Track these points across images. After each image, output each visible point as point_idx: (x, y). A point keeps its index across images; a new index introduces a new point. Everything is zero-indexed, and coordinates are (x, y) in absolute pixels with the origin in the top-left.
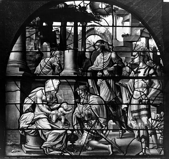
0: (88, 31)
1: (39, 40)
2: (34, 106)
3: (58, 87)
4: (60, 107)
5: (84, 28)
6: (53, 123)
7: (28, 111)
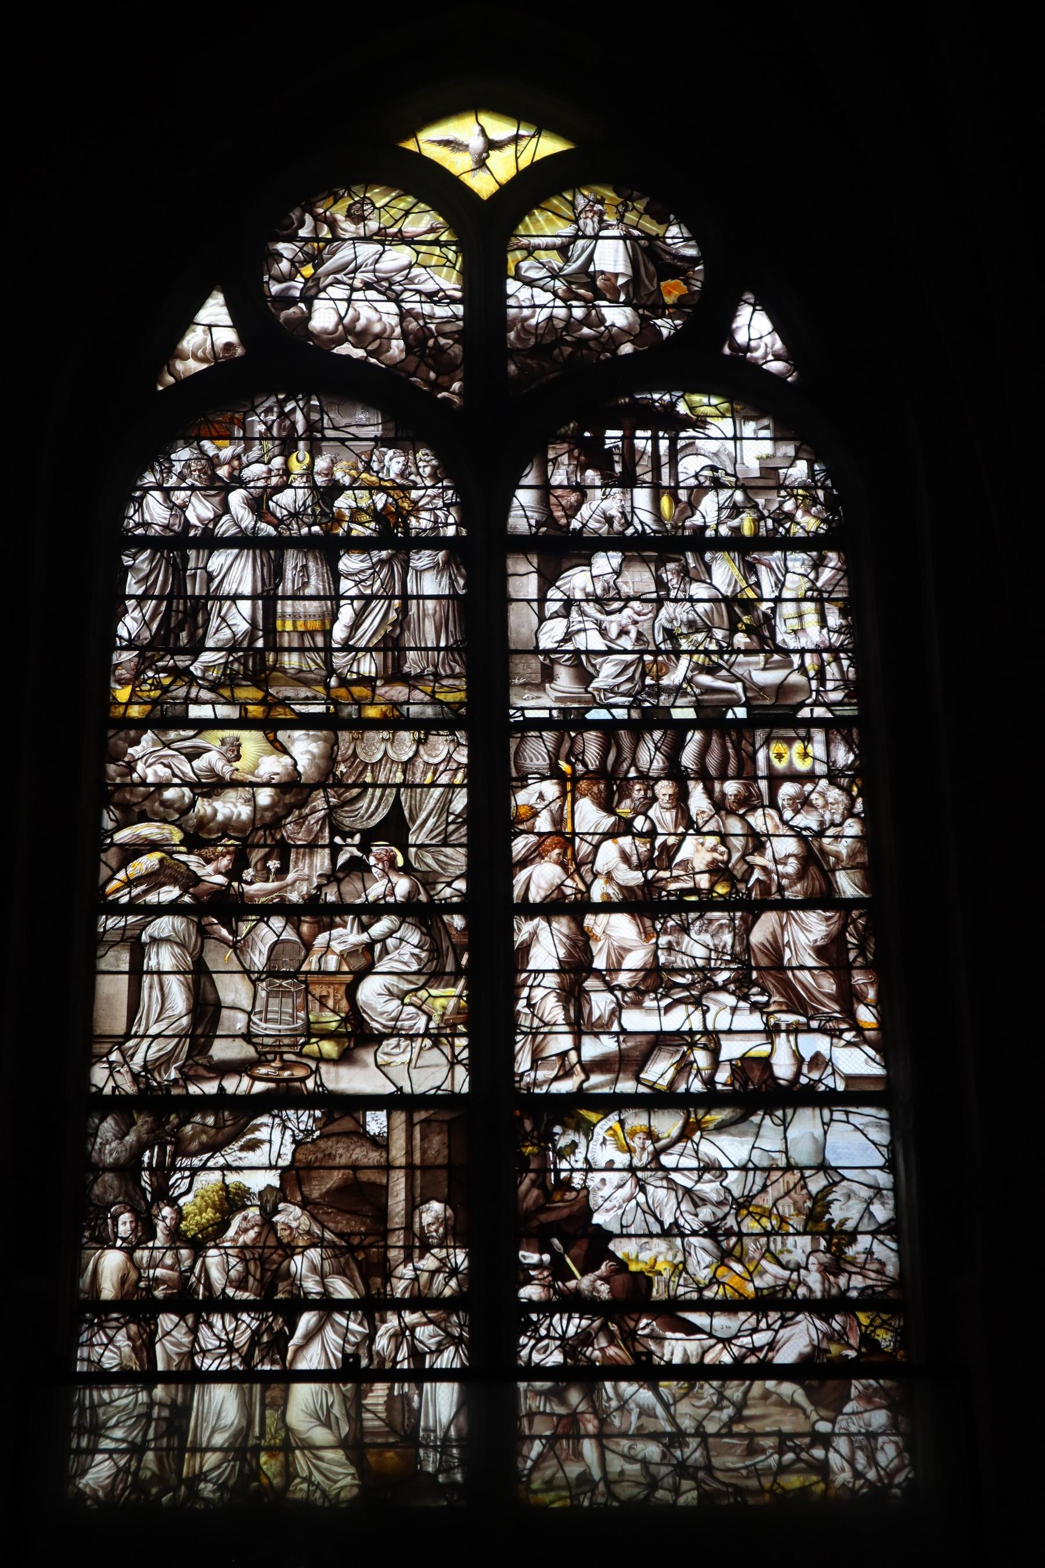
0: (683, 448)
1: (576, 466)
2: (569, 603)
3: (621, 565)
4: (625, 606)
6: (612, 641)
7: (556, 615)
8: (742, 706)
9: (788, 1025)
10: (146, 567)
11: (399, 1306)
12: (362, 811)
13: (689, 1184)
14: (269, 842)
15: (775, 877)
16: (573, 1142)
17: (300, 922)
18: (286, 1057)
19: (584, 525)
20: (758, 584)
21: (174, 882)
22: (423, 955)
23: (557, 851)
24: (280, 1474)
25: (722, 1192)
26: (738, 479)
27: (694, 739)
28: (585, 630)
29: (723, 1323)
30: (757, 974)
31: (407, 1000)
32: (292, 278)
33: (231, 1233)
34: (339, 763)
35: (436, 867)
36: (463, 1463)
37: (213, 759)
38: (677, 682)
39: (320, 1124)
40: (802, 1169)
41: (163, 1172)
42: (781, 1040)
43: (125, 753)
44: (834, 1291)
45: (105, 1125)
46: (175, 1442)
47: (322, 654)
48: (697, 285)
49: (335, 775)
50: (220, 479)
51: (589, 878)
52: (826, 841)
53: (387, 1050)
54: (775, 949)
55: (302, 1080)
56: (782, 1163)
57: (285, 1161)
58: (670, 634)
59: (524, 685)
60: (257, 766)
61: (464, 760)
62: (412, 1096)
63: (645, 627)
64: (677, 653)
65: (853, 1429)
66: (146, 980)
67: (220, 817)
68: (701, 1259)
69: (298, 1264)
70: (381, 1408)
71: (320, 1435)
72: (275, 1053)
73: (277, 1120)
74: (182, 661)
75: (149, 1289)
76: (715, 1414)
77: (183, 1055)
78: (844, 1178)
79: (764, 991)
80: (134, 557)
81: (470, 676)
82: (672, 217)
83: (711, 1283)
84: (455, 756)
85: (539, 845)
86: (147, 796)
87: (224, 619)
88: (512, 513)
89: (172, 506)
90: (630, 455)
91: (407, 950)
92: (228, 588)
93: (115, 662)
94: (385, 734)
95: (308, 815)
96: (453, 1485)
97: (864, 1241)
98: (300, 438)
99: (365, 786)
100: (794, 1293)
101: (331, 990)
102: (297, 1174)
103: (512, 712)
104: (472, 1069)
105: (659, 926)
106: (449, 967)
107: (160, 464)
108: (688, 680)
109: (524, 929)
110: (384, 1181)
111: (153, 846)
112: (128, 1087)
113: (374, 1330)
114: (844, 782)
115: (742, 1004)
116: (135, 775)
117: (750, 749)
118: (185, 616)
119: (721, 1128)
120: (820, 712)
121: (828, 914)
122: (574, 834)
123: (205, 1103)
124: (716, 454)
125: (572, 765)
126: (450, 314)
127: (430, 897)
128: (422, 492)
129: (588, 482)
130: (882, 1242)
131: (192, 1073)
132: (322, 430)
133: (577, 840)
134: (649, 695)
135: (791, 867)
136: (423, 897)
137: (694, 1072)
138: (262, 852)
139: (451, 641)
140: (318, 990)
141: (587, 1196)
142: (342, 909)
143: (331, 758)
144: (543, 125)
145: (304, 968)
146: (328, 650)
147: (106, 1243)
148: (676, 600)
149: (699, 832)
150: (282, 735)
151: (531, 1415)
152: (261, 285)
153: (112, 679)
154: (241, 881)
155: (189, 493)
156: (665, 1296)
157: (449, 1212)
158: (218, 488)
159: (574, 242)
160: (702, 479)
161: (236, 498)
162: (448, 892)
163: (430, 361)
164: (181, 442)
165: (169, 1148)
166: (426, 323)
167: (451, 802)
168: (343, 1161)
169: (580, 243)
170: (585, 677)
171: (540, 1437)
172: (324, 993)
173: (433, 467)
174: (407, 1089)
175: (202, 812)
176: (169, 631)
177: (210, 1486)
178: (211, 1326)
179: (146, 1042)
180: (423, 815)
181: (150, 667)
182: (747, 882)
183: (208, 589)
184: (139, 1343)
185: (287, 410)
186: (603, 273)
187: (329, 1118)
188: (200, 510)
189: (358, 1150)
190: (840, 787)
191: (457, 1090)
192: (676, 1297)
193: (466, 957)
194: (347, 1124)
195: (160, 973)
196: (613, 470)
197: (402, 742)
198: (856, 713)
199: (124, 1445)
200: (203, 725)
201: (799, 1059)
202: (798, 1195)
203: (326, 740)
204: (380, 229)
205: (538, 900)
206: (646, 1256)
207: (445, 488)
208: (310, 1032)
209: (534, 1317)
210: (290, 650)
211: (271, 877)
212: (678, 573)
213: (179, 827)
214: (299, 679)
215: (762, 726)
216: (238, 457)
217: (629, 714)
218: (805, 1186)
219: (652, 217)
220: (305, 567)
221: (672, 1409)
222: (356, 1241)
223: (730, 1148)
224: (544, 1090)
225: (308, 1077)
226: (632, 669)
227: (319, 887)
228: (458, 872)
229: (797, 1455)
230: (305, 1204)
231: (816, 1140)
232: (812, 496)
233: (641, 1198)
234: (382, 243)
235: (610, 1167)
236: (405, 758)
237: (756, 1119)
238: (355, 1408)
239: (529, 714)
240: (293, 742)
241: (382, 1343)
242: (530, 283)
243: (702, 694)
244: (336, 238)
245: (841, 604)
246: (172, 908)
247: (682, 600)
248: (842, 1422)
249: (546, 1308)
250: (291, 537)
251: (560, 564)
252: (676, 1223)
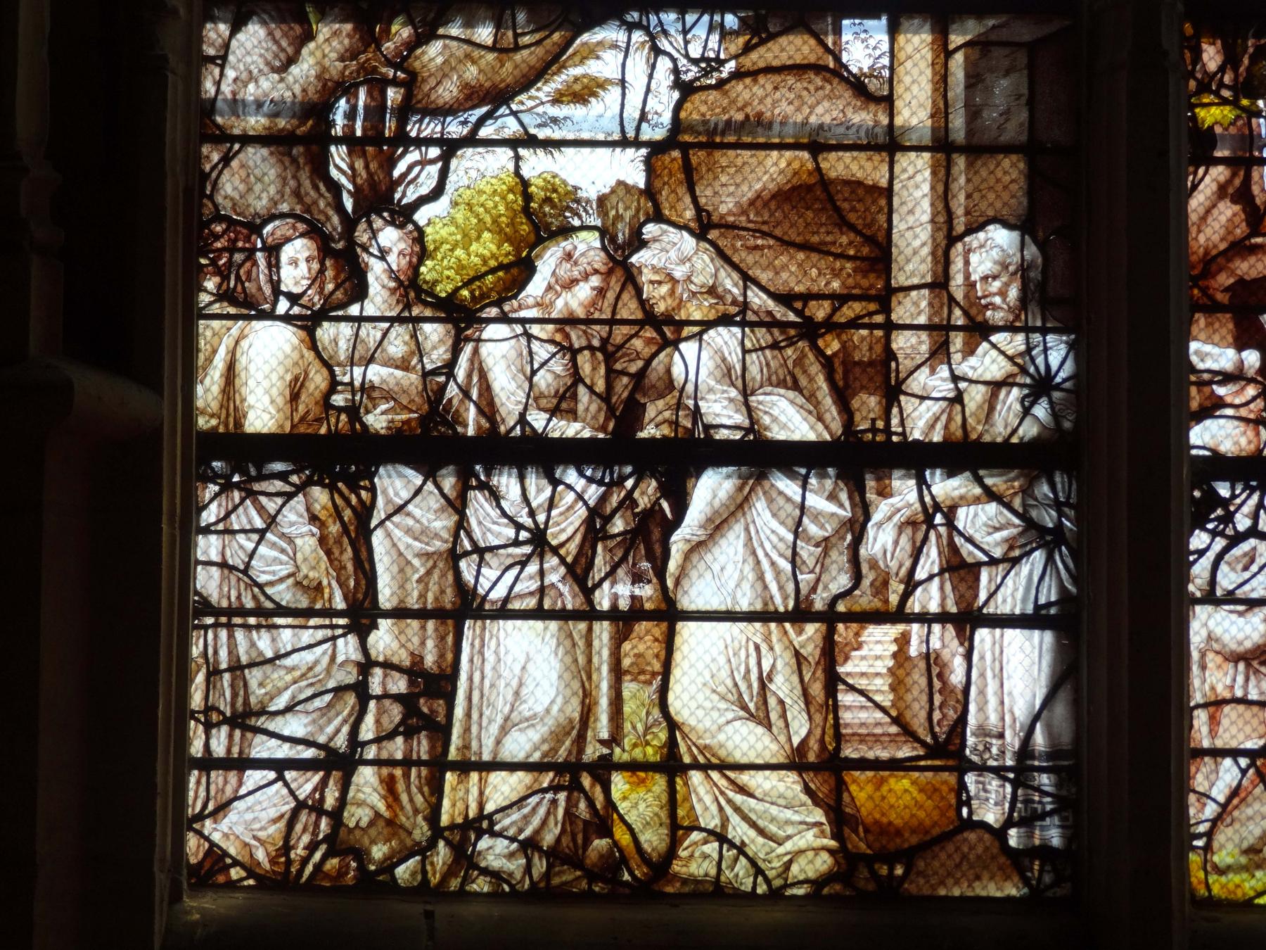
11: (920, 458)
33: (536, 288)
36: (1064, 805)
41: (380, 145)
46: (422, 747)
71: (746, 741)
73: (638, 36)
75: (353, 411)
96: (1044, 851)
113: (864, 511)
151: (1216, 704)
157: (1032, 251)
171: (1235, 753)
177: (501, 845)
178: (495, 496)
199: (309, 753)
230: (704, 226)
241: (882, 540)
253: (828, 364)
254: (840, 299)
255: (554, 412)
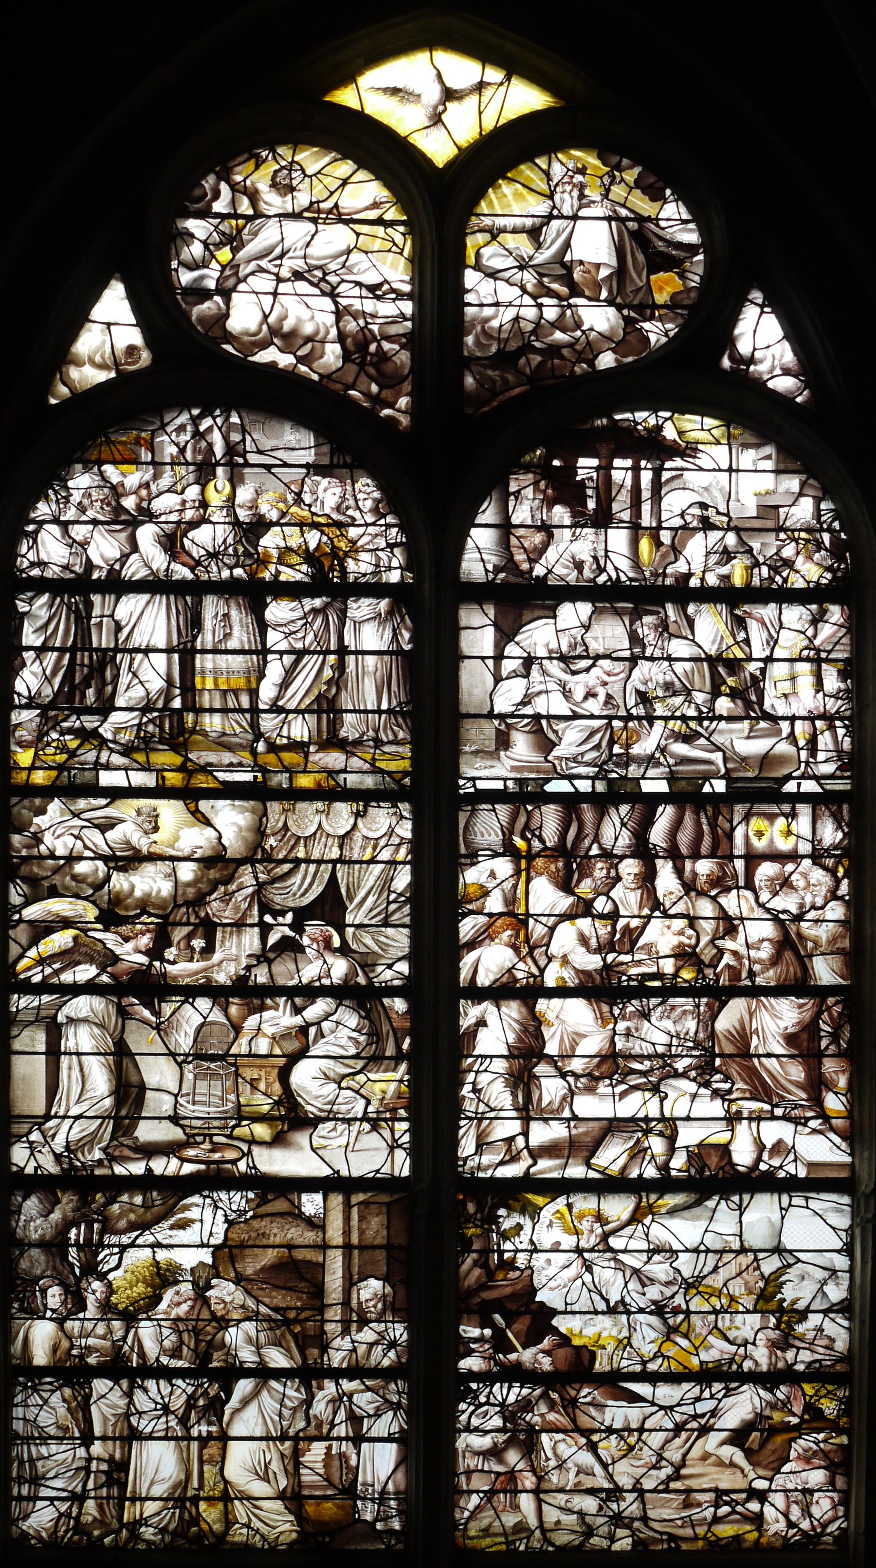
0: (669, 481)
1: (543, 501)
2: (529, 661)
3: (590, 618)
4: (593, 665)
5: (657, 472)
6: (576, 704)
7: (514, 674)
8: (722, 778)
9: (751, 1112)
10: (44, 614)
11: (336, 1374)
12: (295, 888)
13: (638, 1265)
14: (192, 920)
15: (747, 962)
16: (518, 1224)
17: (228, 1003)
18: (216, 1139)
19: (550, 571)
20: (747, 641)
21: (91, 960)
22: (362, 1038)
23: (509, 932)
24: (220, 1521)
25: (671, 1271)
26: (730, 519)
27: (665, 816)
28: (547, 692)
29: (666, 1393)
30: (719, 1061)
31: (344, 1084)
32: (205, 264)
33: (163, 1306)
34: (268, 836)
35: (376, 948)
36: (400, 1513)
37: (128, 832)
38: (649, 752)
39: (253, 1205)
40: (755, 1251)
41: (90, 1248)
42: (742, 1128)
43: (31, 823)
44: (781, 1365)
45: (28, 1202)
46: (115, 1492)
47: (248, 716)
48: (695, 280)
49: (264, 849)
50: (127, 512)
51: (542, 962)
52: (803, 924)
53: (322, 1133)
54: (742, 1037)
55: (234, 1162)
56: (736, 1245)
57: (218, 1240)
58: (643, 698)
59: (476, 753)
60: (177, 838)
61: (408, 835)
62: (350, 1179)
63: (615, 689)
64: (651, 719)
65: (790, 1486)
66: (64, 1061)
67: (138, 893)
68: (647, 1334)
69: (233, 1336)
70: (320, 1465)
71: (259, 1488)
72: (205, 1135)
73: (208, 1201)
74: (90, 722)
75: (81, 1357)
76: (653, 1472)
77: (107, 1136)
78: (799, 1260)
79: (727, 1078)
80: (30, 601)
81: (416, 743)
82: (668, 192)
83: (655, 1357)
84: (398, 830)
85: (489, 926)
86: (57, 870)
87: (135, 675)
88: (466, 557)
89: (72, 543)
90: (606, 490)
91: (344, 1033)
92: (138, 640)
93: (14, 721)
94: (320, 805)
95: (234, 892)
96: (391, 1532)
97: (814, 1320)
98: (218, 464)
99: (297, 862)
100: (740, 1366)
101: (263, 1073)
102: (230, 1252)
103: (461, 782)
104: (414, 1152)
105: (616, 1011)
106: (390, 1051)
107: (56, 492)
108: (663, 750)
109: (470, 1013)
110: (321, 1259)
111: (66, 923)
112: (50, 1166)
114: (829, 862)
115: (703, 1091)
116: (42, 847)
117: (727, 825)
118: (91, 671)
119: (673, 1212)
120: (809, 786)
121: (801, 1001)
122: (528, 915)
123: (131, 1183)
124: (706, 489)
125: (528, 841)
126: (397, 312)
127: (370, 979)
128: (361, 530)
129: (556, 521)
130: (833, 1320)
131: (117, 1153)
132: (243, 455)
133: (531, 921)
134: (617, 765)
135: (765, 952)
136: (361, 980)
137: (648, 1158)
138: (186, 930)
139: (394, 703)
140: (248, 1073)
141: (531, 1276)
142: (273, 991)
143: (260, 832)
144: (514, 68)
145: (234, 1051)
146: (255, 711)
147: (36, 1313)
148: (652, 659)
149: (666, 915)
150: (204, 805)
151: (469, 1473)
152: (167, 273)
153: (12, 741)
154: (163, 960)
155: (90, 527)
156: (607, 1368)
157: (388, 1289)
158: (126, 521)
159: (548, 224)
160: (688, 518)
161: (146, 534)
162: (388, 974)
163: (372, 371)
164: (79, 467)
165: (96, 1226)
166: (367, 323)
167: (392, 879)
168: (278, 1240)
169: (555, 224)
170: (546, 745)
171: (478, 1492)
172: (256, 1076)
173: (374, 500)
174: (344, 1173)
175: (118, 887)
176: (73, 688)
177: (151, 1530)
178: (146, 1391)
179: (68, 1122)
180: (362, 893)
181: (53, 728)
182: (716, 967)
183: (117, 640)
184: (74, 1404)
185: (202, 428)
186: (581, 263)
187: (263, 1200)
188: (104, 548)
189: (293, 1230)
190: (824, 868)
191: (396, 1174)
192: (619, 1369)
193: (408, 1041)
194: (280, 1205)
195: (78, 1054)
196: (585, 506)
197: (339, 814)
198: (848, 787)
199: (65, 1494)
200: (115, 794)
201: (760, 1147)
202: (751, 1277)
203: (253, 811)
204: (312, 203)
205: (487, 983)
206: (590, 1332)
207: (388, 526)
208: (240, 1115)
209: (474, 1386)
210: (212, 710)
211: (196, 956)
212: (656, 627)
213: (94, 903)
214: (222, 743)
215: (742, 801)
216: (147, 485)
217: (593, 786)
218: (758, 1268)
219: (644, 193)
220: (226, 616)
221: (610, 1468)
222: (292, 1315)
223: (684, 1230)
224: (489, 1173)
225: (239, 1159)
226: (599, 735)
227: (248, 968)
228: (400, 954)
229: (733, 1508)
230: (239, 1280)
231: (772, 1224)
232: (816, 540)
233: (587, 1277)
234: (314, 221)
235: (556, 1248)
236: (342, 832)
237: (711, 1204)
238: (294, 1463)
239: (481, 785)
240: (216, 813)
241: (320, 1407)
242: (493, 274)
243: (676, 764)
244: (258, 215)
245: (840, 665)
246: (90, 988)
247: (659, 659)
248: (779, 1481)
249: (487, 1378)
250: (209, 582)
251: (520, 616)
252: (622, 1301)
253: (295, 1336)
254: (302, 1309)
255: (172, 1357)
